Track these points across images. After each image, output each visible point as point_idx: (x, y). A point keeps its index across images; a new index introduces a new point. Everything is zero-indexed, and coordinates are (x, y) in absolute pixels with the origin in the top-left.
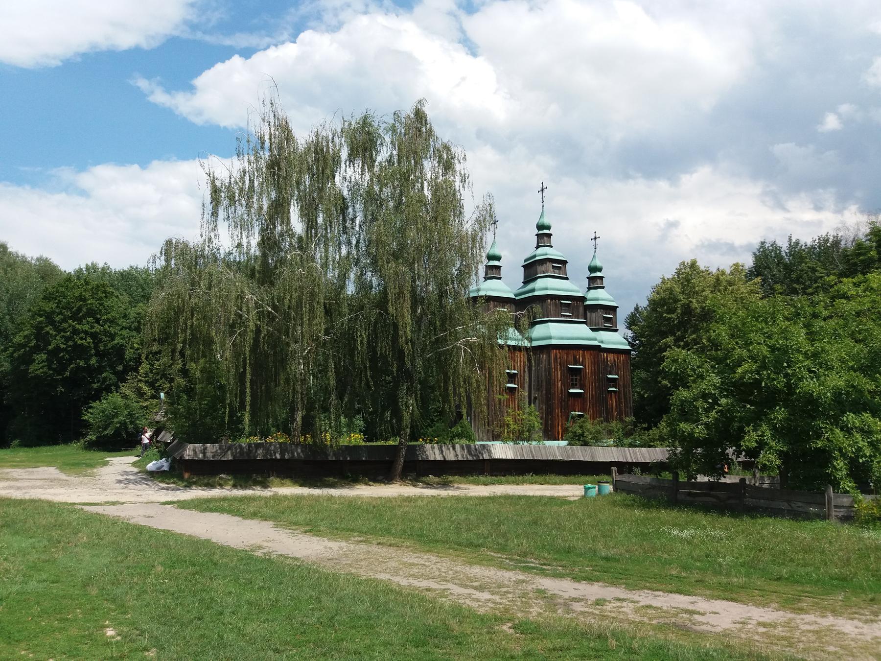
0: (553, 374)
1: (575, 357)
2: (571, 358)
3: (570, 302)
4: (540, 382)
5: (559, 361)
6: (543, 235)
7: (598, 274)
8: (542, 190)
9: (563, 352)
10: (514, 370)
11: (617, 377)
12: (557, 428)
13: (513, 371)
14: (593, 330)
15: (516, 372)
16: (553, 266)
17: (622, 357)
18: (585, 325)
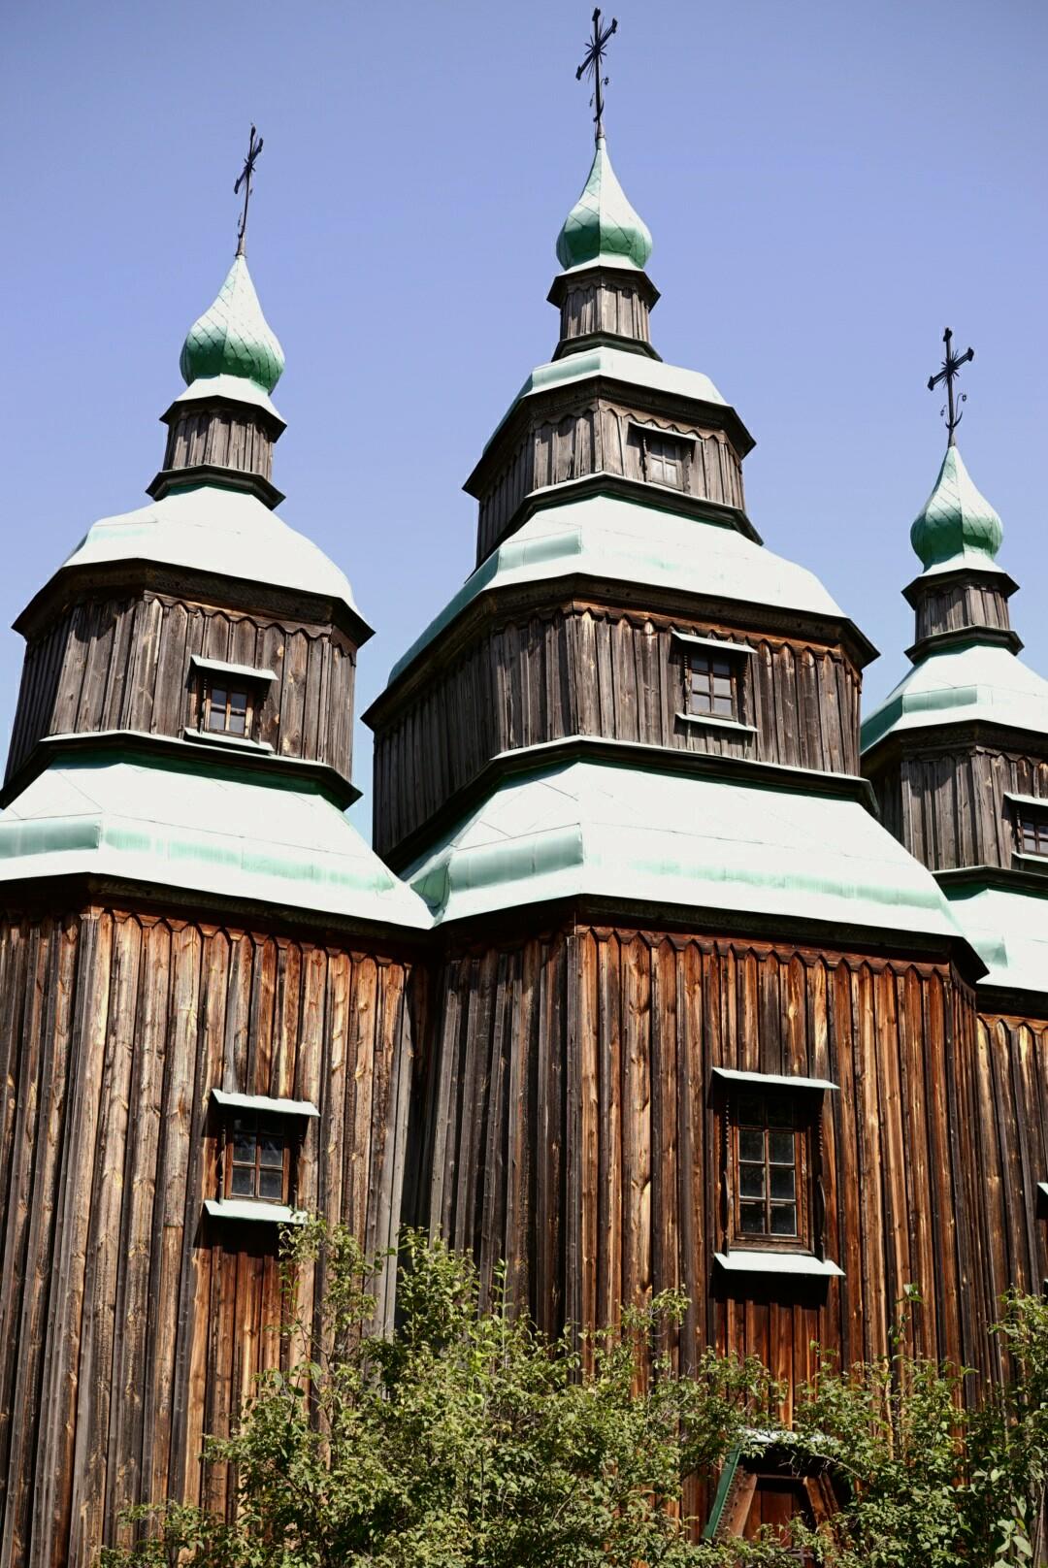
0: (589, 1123)
1: (770, 1017)
2: (737, 1016)
4: (492, 1193)
5: (638, 1025)
10: (296, 1094)
13: (284, 1106)
15: (308, 1108)
18: (854, 810)
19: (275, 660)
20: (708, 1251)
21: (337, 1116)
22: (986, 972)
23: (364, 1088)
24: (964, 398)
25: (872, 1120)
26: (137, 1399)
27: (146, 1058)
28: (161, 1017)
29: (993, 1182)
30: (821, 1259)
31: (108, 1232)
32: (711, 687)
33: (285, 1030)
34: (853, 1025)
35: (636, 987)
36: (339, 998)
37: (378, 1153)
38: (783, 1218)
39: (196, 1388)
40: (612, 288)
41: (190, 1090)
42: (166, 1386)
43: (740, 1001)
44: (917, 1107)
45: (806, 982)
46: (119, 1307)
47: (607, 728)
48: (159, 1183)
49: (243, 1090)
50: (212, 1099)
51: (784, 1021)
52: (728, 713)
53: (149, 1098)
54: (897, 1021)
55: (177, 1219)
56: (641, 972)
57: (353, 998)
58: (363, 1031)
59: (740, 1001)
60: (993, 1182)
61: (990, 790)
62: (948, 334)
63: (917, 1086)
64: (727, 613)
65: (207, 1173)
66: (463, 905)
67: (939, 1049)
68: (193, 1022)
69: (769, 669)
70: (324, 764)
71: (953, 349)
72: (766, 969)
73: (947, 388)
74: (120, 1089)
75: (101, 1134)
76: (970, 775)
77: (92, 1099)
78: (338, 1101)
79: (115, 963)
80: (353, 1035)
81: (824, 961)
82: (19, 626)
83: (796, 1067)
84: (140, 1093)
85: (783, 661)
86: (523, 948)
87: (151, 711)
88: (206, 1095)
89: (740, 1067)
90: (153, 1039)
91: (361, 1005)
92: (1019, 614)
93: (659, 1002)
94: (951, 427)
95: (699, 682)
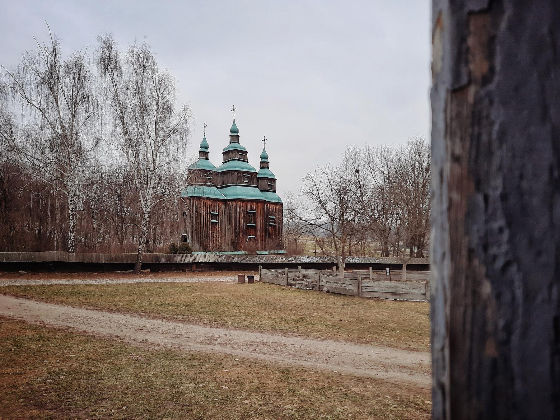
1: (251, 206)
2: (249, 207)
3: (249, 175)
5: (242, 208)
6: (235, 136)
7: (266, 160)
8: (234, 110)
9: (244, 204)
10: (216, 212)
12: (240, 245)
14: (261, 191)
15: (217, 213)
16: (239, 154)
18: (257, 188)
23: (221, 211)
25: (258, 214)
29: (266, 216)
37: (222, 216)
48: (207, 219)
63: (261, 211)
74: (204, 212)
75: (203, 216)
77: (203, 213)
90: (206, 209)
94: (264, 146)
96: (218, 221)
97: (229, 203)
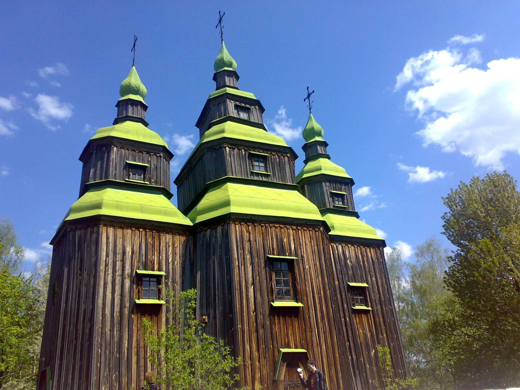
0: (236, 271)
2: (272, 242)
5: (247, 246)
10: (160, 270)
11: (365, 285)
15: (163, 273)
17: (371, 253)
18: (296, 192)
19: (149, 162)
20: (269, 302)
21: (171, 275)
22: (330, 231)
24: (313, 102)
25: (307, 267)
26: (118, 355)
27: (117, 262)
28: (121, 251)
29: (337, 283)
30: (297, 303)
31: (108, 311)
32: (259, 165)
33: (156, 253)
34: (300, 243)
35: (246, 235)
36: (170, 244)
38: (287, 293)
39: (134, 351)
40: (229, 76)
41: (130, 270)
42: (126, 351)
43: (272, 238)
44: (318, 263)
45: (288, 233)
46: (112, 330)
47: (234, 174)
48: (122, 295)
49: (145, 270)
50: (136, 272)
51: (283, 243)
52: (264, 170)
53: (119, 273)
54: (311, 242)
55: (128, 305)
56: (247, 232)
57: (173, 245)
58: (177, 252)
59: (272, 238)
60: (337, 283)
61: (327, 190)
62: (308, 88)
63: (317, 258)
64: (262, 147)
65: (136, 291)
66: (201, 219)
67: (322, 248)
68: (130, 252)
69: (273, 160)
70: (163, 187)
71: (309, 91)
72: (278, 230)
73: (308, 101)
74: (110, 271)
75: (105, 284)
76: (322, 187)
77: (102, 274)
78: (171, 271)
79: (108, 238)
80: (174, 254)
81: (292, 228)
82: (80, 159)
83: (287, 254)
84: (116, 272)
85: (276, 158)
86: (217, 228)
87: (115, 174)
88: (134, 272)
89: (273, 254)
90: (119, 257)
91: (176, 246)
92: (329, 150)
93: (251, 239)
94: (310, 109)
95: (256, 164)
96: (167, 302)
97: (205, 235)
